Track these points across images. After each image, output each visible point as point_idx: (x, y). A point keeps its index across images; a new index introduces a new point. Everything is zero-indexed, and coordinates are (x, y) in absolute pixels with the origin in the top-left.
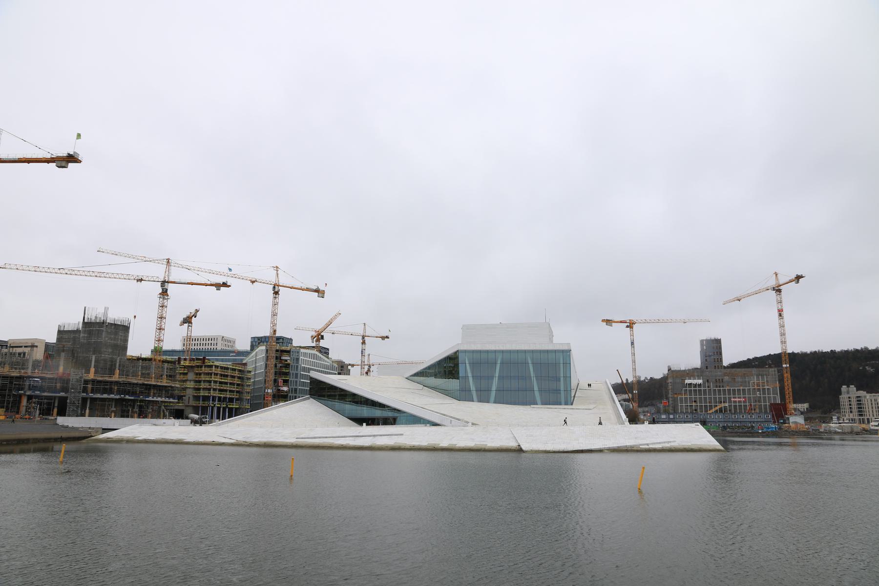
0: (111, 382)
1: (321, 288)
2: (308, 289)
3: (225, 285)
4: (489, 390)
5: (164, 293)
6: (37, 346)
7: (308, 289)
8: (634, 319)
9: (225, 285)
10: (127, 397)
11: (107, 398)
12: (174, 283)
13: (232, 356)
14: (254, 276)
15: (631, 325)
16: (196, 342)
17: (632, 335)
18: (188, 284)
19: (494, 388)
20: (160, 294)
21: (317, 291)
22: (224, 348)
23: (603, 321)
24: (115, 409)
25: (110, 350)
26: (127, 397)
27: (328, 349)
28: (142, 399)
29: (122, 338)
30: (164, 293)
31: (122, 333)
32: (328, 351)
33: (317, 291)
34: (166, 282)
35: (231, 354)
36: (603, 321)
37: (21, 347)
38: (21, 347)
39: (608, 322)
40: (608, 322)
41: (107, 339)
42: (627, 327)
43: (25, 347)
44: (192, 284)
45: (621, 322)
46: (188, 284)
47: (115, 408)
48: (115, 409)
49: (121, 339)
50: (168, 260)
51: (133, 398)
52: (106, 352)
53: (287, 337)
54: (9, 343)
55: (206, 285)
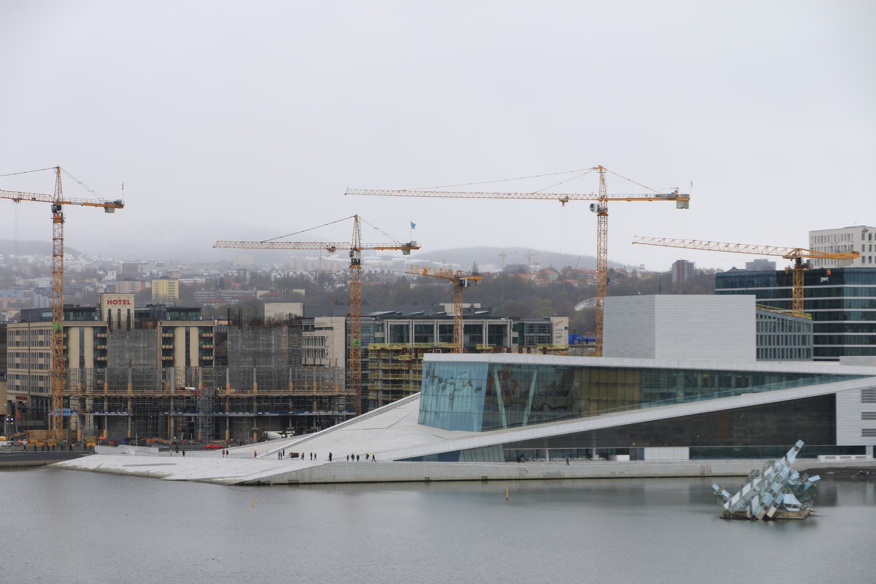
0: (250, 399)
1: (681, 192)
2: (659, 197)
7: (659, 197)
10: (267, 414)
11: (243, 417)
13: (825, 283)
14: (563, 191)
24: (257, 429)
25: (250, 359)
26: (267, 414)
28: (293, 415)
29: (265, 343)
31: (263, 337)
37: (321, 329)
41: (244, 346)
47: (257, 427)
48: (257, 429)
49: (263, 344)
51: (277, 415)
52: (244, 362)
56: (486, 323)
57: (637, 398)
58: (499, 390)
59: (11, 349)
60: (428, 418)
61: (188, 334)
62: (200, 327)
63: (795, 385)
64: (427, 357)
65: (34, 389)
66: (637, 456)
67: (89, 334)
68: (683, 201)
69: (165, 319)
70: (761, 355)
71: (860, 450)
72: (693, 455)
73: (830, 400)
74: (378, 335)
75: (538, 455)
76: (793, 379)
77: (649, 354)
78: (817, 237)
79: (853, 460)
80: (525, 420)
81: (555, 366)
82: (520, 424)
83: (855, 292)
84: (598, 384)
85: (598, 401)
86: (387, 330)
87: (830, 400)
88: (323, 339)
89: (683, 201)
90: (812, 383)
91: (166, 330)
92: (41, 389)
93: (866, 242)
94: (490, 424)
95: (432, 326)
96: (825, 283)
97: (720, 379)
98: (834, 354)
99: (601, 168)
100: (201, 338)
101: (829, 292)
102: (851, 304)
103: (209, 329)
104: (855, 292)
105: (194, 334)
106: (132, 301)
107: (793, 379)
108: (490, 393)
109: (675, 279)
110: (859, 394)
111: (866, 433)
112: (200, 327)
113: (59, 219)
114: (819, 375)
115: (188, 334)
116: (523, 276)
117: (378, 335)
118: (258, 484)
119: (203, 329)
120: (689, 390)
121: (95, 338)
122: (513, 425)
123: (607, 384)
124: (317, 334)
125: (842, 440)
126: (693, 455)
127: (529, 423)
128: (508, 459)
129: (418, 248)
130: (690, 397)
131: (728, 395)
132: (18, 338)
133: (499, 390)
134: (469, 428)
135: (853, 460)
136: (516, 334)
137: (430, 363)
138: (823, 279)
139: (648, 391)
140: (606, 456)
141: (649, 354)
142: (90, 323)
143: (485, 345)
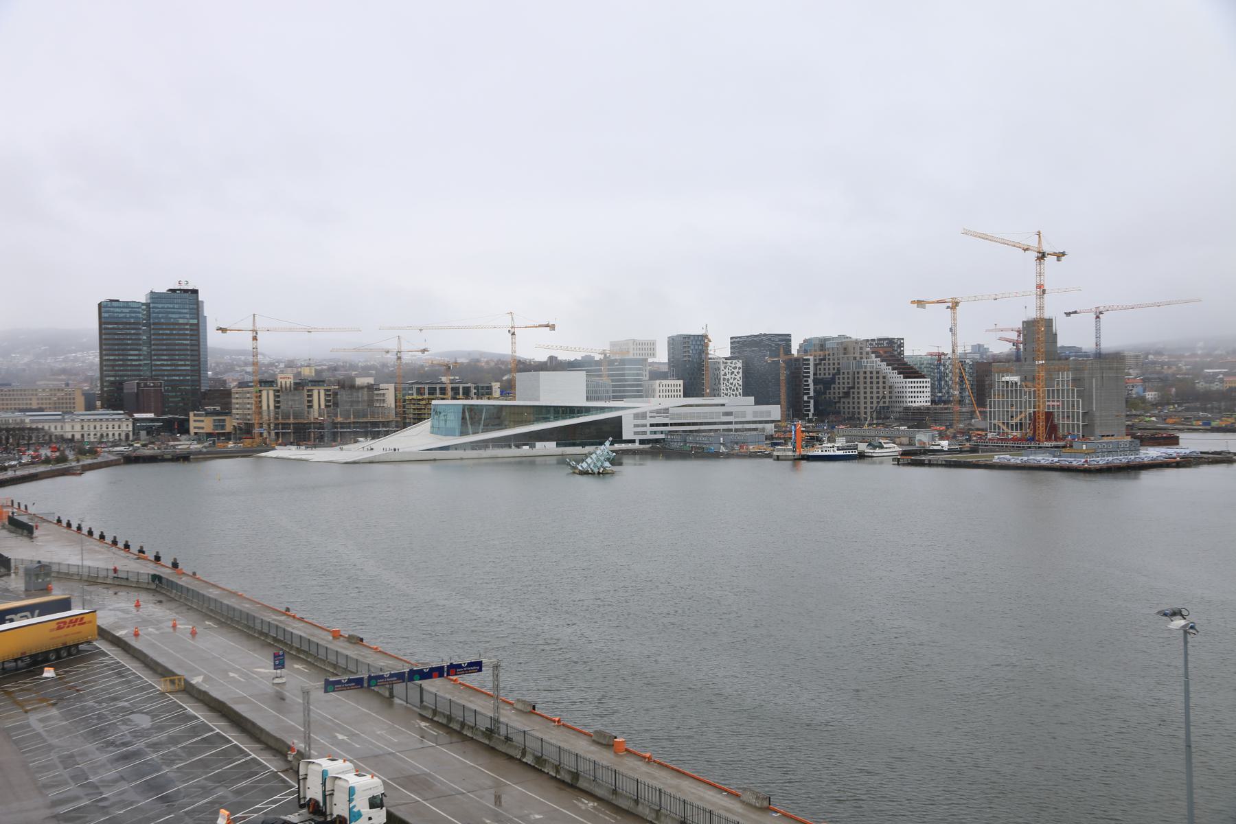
0: (350, 423)
1: (550, 324)
2: (540, 326)
7: (540, 326)
8: (958, 296)
10: (358, 430)
13: (617, 365)
15: (955, 305)
17: (954, 319)
21: (547, 326)
23: (913, 302)
25: (349, 404)
26: (358, 430)
27: (789, 335)
32: (788, 338)
33: (547, 326)
36: (913, 302)
39: (920, 303)
40: (920, 303)
42: (948, 307)
45: (938, 302)
53: (697, 334)
56: (461, 386)
57: (532, 420)
58: (468, 417)
59: (234, 401)
60: (435, 431)
61: (319, 393)
62: (325, 390)
63: (604, 412)
64: (434, 402)
65: (246, 419)
66: (532, 446)
67: (271, 393)
68: (552, 327)
69: (308, 386)
70: (588, 399)
71: (633, 441)
72: (558, 445)
73: (619, 419)
74: (410, 392)
75: (486, 447)
76: (602, 409)
77: (538, 399)
78: (613, 344)
79: (630, 446)
80: (481, 431)
81: (494, 405)
82: (478, 433)
83: (630, 369)
84: (514, 413)
85: (514, 421)
86: (415, 390)
87: (619, 419)
88: (384, 394)
89: (552, 327)
90: (611, 411)
91: (308, 391)
92: (249, 420)
94: (463, 433)
95: (436, 388)
96: (617, 365)
97: (570, 410)
98: (621, 398)
100: (326, 395)
101: (618, 370)
102: (629, 375)
103: (329, 390)
104: (630, 369)
106: (292, 377)
107: (602, 409)
108: (464, 418)
109: (549, 364)
110: (632, 416)
111: (636, 433)
112: (325, 390)
113: (255, 338)
114: (615, 407)
115: (319, 393)
116: (478, 364)
117: (410, 392)
118: (354, 463)
119: (327, 390)
120: (556, 415)
121: (275, 395)
122: (474, 433)
123: (518, 413)
124: (381, 392)
126: (558, 445)
127: (482, 432)
128: (473, 449)
130: (556, 419)
131: (574, 417)
132: (237, 396)
133: (468, 417)
134: (454, 435)
135: (630, 446)
136: (476, 391)
137: (435, 405)
138: (616, 364)
139: (537, 416)
140: (518, 446)
141: (538, 399)
142: (272, 388)
143: (461, 396)
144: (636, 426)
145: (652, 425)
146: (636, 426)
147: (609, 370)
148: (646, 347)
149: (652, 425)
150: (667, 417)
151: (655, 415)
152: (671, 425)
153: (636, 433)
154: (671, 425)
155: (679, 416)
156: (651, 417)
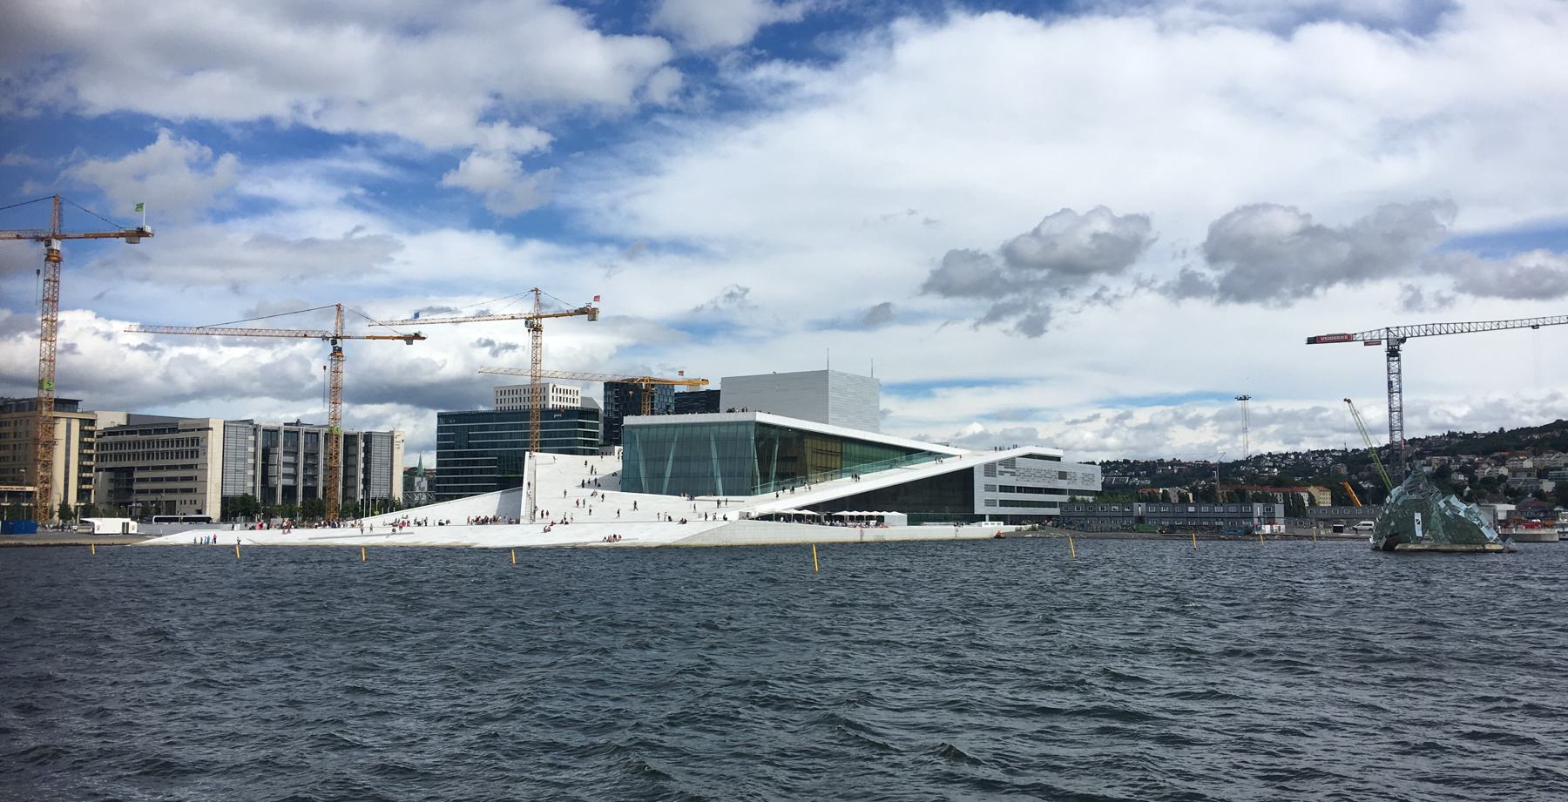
3: (417, 336)
4: (662, 476)
5: (337, 352)
6: (212, 429)
9: (417, 336)
12: (349, 337)
13: (557, 418)
16: (515, 396)
18: (368, 338)
19: (668, 474)
20: (331, 355)
22: (559, 403)
30: (337, 352)
34: (339, 338)
35: (555, 416)
37: (193, 430)
38: (193, 430)
43: (199, 430)
44: (374, 338)
46: (368, 338)
50: (339, 306)
54: (180, 423)
55: (393, 338)
61: (69, 426)
90: (910, 461)
93: (554, 394)
96: (557, 418)
99: (537, 290)
105: (76, 425)
111: (990, 503)
115: (69, 426)
116: (1186, 272)
125: (979, 508)
129: (424, 338)
137: (633, 427)
144: (990, 488)
145: (1004, 489)
146: (990, 488)
147: (542, 426)
148: (569, 396)
149: (1004, 489)
150: (1013, 474)
151: (1002, 468)
152: (1020, 489)
153: (990, 503)
154: (1020, 489)
155: (1027, 473)
156: (1002, 473)
